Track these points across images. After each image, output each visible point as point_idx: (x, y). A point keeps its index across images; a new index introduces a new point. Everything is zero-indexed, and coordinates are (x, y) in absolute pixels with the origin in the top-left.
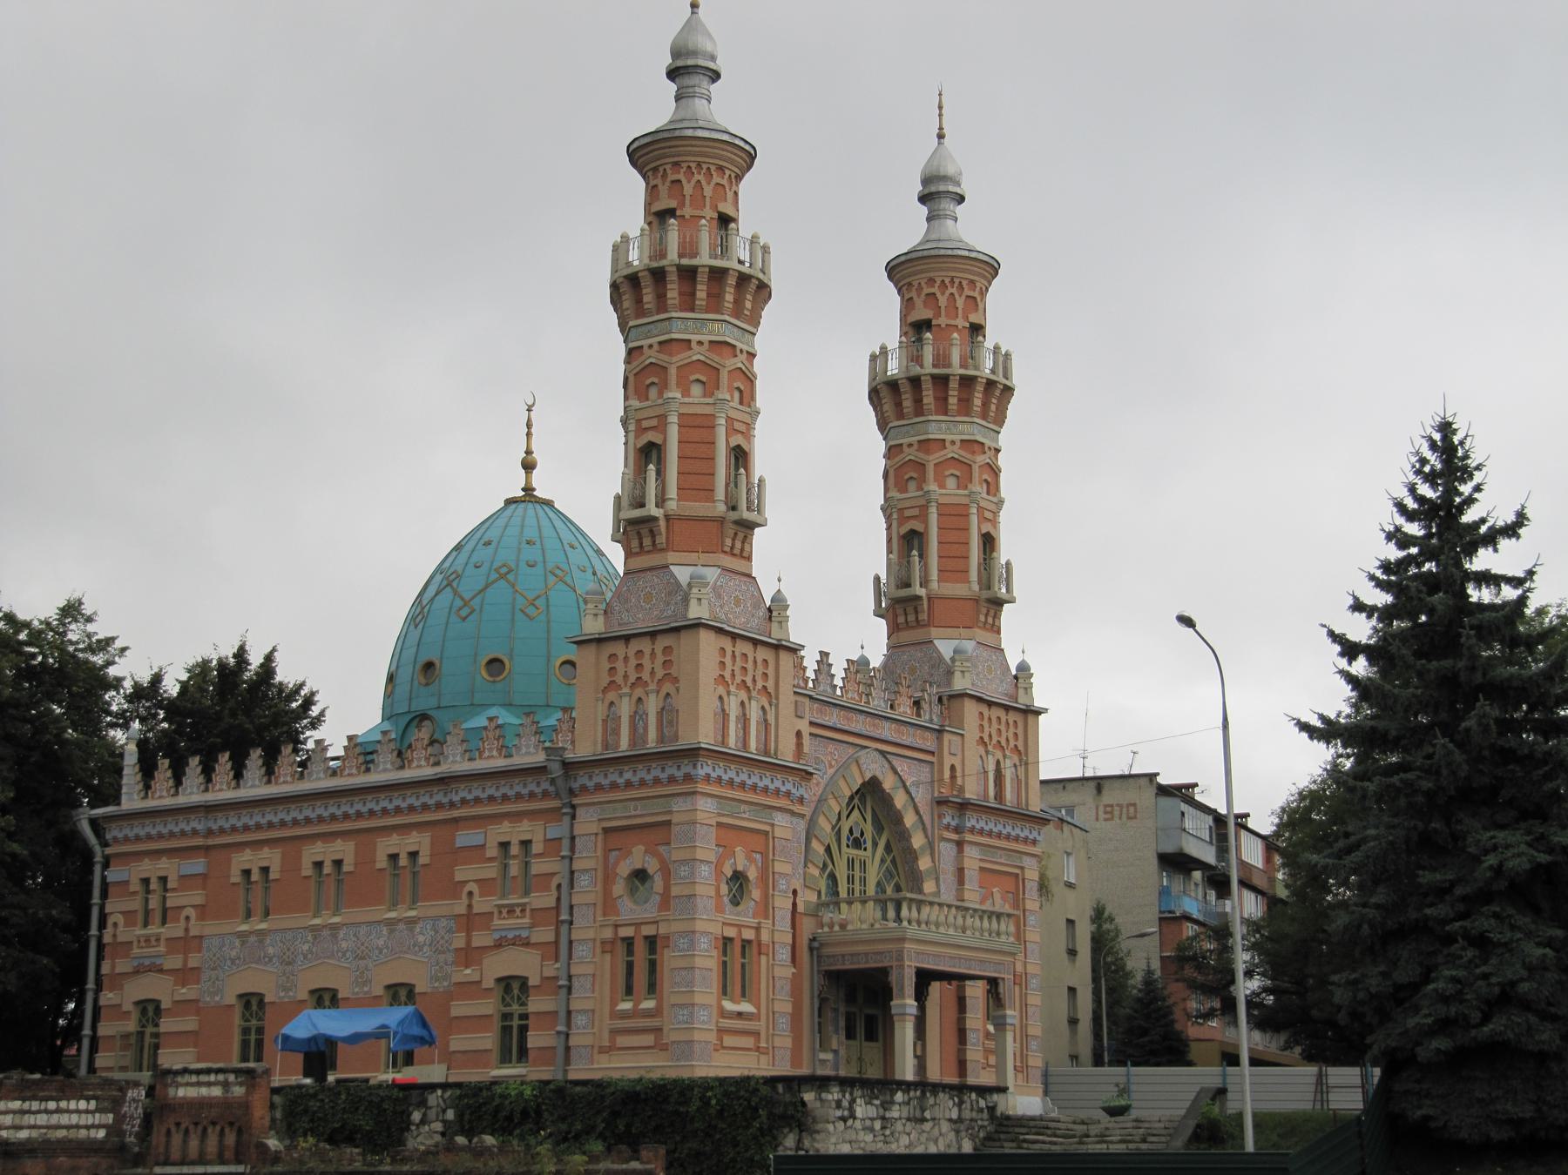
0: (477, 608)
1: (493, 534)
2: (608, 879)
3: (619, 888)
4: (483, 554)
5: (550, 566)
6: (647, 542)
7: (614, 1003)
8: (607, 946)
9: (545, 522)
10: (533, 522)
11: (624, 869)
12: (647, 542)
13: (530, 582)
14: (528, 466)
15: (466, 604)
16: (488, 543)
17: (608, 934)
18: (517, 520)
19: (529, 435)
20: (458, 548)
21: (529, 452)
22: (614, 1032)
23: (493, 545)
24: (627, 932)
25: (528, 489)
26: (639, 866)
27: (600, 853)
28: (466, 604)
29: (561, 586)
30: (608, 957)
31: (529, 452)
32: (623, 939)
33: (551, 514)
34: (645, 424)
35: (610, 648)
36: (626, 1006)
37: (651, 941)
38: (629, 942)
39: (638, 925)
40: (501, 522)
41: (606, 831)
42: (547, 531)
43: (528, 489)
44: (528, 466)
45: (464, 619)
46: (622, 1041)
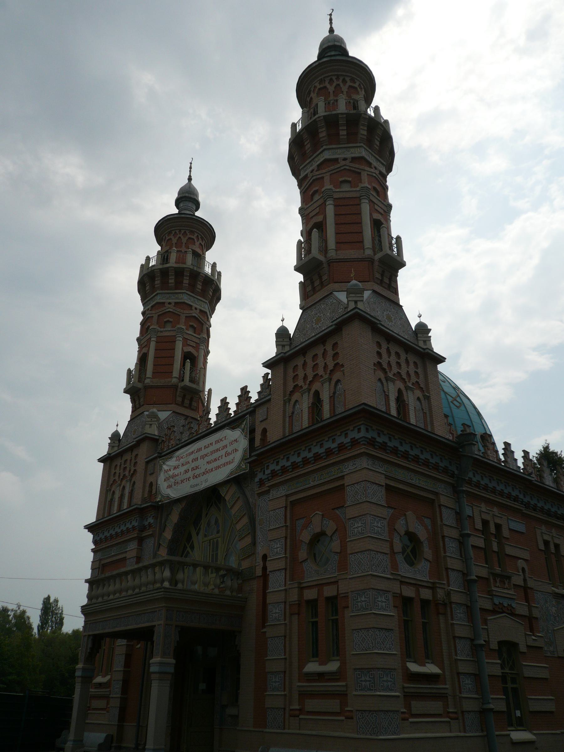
7: (301, 666)
11: (306, 536)
22: (304, 695)
24: (310, 594)
32: (308, 602)
34: (312, 215)
36: (312, 667)
37: (332, 601)
39: (320, 586)
46: (311, 704)
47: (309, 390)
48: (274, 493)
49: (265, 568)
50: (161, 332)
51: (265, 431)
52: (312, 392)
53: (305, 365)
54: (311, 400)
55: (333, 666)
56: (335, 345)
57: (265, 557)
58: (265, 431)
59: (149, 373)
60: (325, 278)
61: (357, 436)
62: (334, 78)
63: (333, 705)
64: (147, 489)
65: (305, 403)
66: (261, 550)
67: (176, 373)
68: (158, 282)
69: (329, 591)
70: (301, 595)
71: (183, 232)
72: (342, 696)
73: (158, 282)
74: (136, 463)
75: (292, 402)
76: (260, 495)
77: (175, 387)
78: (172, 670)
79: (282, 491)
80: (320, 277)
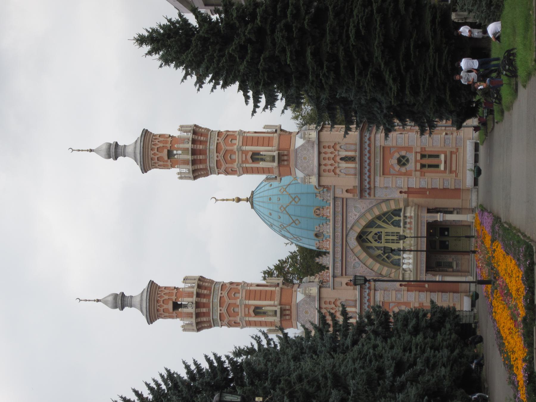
0: (296, 218)
1: (267, 212)
2: (401, 174)
3: (403, 170)
4: (275, 215)
5: (279, 193)
6: (285, 158)
8: (423, 174)
9: (261, 195)
10: (261, 199)
11: (397, 167)
12: (285, 158)
13: (286, 200)
14: (239, 200)
15: (294, 222)
16: (271, 214)
17: (418, 173)
18: (261, 204)
19: (227, 200)
20: (271, 226)
21: (234, 200)
23: (272, 212)
24: (418, 167)
25: (247, 200)
26: (396, 162)
27: (391, 176)
28: (294, 222)
29: (287, 190)
30: (426, 174)
31: (234, 200)
33: (258, 192)
34: (244, 159)
35: (322, 171)
36: (442, 167)
38: (423, 166)
40: (262, 210)
41: (383, 174)
42: (266, 194)
43: (247, 200)
44: (239, 200)
45: (300, 222)
46: (454, 168)
47: (339, 163)
48: (377, 184)
49: (405, 192)
50: (242, 297)
51: (347, 191)
52: (339, 161)
53: (325, 165)
54: (343, 162)
55: (442, 157)
56: (324, 147)
57: (401, 192)
58: (347, 191)
59: (272, 303)
60: (286, 153)
61: (368, 137)
62: (153, 143)
63: (454, 156)
64: (349, 287)
65: (343, 165)
66: (397, 195)
67: (273, 289)
68: (204, 300)
69: (419, 157)
70: (418, 171)
71: (159, 292)
72: (452, 153)
73: (204, 300)
74: (330, 303)
75: (339, 173)
76: (374, 196)
77: (282, 289)
78: (442, 214)
79: (378, 179)
80: (284, 155)
